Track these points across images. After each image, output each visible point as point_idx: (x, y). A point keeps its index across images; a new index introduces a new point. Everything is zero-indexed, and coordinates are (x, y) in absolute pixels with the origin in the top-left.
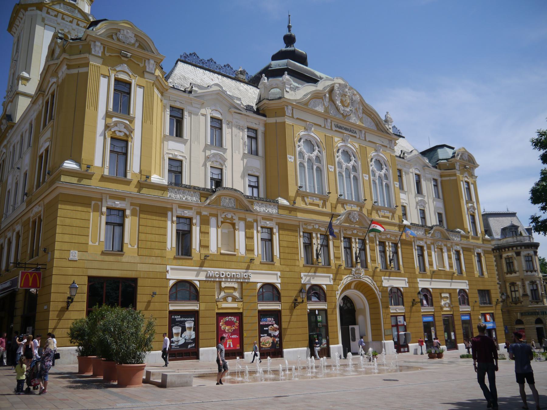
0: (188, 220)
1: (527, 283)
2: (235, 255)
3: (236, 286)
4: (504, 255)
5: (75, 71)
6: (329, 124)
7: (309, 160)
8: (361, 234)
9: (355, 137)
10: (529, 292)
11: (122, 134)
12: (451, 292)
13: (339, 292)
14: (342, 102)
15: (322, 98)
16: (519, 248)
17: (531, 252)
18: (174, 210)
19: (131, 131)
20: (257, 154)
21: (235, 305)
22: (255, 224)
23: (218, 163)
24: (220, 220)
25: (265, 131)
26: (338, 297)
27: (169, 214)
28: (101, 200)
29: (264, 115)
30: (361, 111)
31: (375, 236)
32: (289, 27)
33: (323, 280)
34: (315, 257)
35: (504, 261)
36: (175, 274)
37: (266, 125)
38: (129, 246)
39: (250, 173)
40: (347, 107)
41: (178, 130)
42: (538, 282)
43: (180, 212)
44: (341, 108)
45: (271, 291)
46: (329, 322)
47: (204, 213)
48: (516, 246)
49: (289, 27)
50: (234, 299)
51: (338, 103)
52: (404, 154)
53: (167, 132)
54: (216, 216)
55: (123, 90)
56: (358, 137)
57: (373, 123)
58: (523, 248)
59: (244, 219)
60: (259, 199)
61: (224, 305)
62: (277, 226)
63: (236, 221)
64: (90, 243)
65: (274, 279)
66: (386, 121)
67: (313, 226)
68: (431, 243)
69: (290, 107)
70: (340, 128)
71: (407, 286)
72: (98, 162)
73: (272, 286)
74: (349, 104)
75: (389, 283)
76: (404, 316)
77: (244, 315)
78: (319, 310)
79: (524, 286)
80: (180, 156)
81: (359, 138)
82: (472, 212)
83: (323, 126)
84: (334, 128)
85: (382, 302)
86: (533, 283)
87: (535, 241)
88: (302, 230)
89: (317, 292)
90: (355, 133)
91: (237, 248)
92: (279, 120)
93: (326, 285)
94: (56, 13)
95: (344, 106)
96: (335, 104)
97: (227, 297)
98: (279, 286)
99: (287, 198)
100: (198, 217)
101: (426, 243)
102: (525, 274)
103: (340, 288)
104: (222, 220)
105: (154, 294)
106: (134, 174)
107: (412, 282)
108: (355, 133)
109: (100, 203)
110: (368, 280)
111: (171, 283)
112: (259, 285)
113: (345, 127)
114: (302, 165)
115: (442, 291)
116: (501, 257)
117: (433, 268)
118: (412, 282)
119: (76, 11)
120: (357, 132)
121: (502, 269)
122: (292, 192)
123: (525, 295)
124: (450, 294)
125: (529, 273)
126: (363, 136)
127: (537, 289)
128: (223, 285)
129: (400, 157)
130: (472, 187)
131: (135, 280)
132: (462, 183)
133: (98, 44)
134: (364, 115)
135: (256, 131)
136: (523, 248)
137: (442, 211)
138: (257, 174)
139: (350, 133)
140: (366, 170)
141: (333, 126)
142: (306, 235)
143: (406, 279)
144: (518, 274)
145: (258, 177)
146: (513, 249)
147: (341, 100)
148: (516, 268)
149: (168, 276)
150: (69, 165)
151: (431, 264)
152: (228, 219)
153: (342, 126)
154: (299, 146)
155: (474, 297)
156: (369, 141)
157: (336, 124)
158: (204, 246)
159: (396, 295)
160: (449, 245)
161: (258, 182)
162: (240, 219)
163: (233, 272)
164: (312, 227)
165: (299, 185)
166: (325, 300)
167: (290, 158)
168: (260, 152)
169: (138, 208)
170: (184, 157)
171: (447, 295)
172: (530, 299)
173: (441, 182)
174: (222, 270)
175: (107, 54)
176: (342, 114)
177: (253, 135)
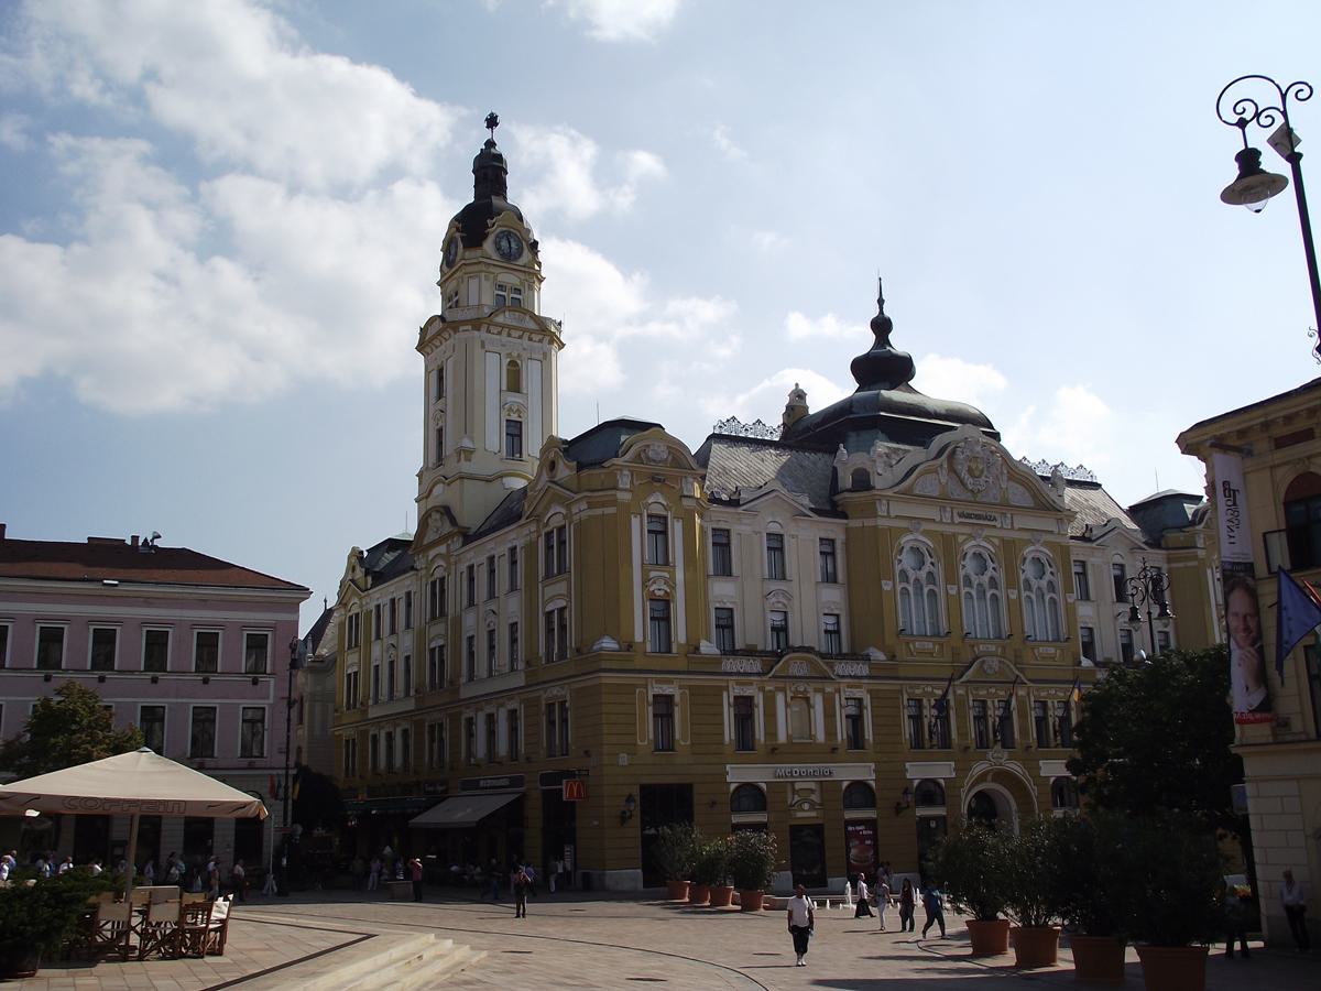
5: (599, 511)
6: (948, 515)
8: (1002, 693)
11: (662, 593)
13: (966, 788)
14: (970, 471)
15: (936, 472)
18: (730, 689)
19: (673, 588)
20: (835, 581)
21: (814, 814)
23: (780, 605)
24: (790, 694)
25: (847, 539)
27: (725, 694)
28: (646, 686)
29: (846, 517)
30: (1005, 478)
31: (1028, 694)
32: (881, 302)
33: (942, 771)
34: (927, 737)
36: (737, 775)
37: (847, 530)
38: (683, 743)
39: (826, 612)
40: (979, 477)
44: (969, 481)
45: (860, 793)
47: (767, 688)
49: (881, 302)
50: (812, 808)
51: (965, 475)
52: (1091, 530)
54: (783, 690)
55: (660, 531)
56: (998, 524)
59: (822, 691)
60: (842, 656)
61: (799, 814)
64: (639, 743)
65: (864, 772)
70: (969, 516)
72: (638, 638)
74: (982, 472)
81: (1002, 528)
84: (957, 520)
88: (906, 697)
89: (930, 793)
90: (995, 519)
91: (813, 733)
92: (869, 523)
94: (500, 329)
95: (973, 476)
96: (959, 476)
98: (873, 784)
100: (761, 696)
103: (967, 783)
105: (714, 803)
106: (679, 645)
109: (645, 691)
110: (1016, 767)
111: (733, 787)
112: (845, 784)
114: (905, 591)
119: (528, 318)
126: (1009, 521)
128: (797, 786)
131: (690, 787)
134: (1011, 483)
135: (832, 541)
138: (836, 612)
141: (955, 514)
142: (912, 703)
145: (837, 616)
147: (969, 467)
150: (608, 644)
152: (801, 693)
156: (1020, 529)
157: (960, 511)
158: (771, 731)
161: (838, 623)
162: (816, 691)
163: (812, 767)
168: (841, 576)
169: (687, 691)
170: (734, 603)
173: (1170, 571)
174: (796, 767)
176: (972, 491)
177: (828, 549)
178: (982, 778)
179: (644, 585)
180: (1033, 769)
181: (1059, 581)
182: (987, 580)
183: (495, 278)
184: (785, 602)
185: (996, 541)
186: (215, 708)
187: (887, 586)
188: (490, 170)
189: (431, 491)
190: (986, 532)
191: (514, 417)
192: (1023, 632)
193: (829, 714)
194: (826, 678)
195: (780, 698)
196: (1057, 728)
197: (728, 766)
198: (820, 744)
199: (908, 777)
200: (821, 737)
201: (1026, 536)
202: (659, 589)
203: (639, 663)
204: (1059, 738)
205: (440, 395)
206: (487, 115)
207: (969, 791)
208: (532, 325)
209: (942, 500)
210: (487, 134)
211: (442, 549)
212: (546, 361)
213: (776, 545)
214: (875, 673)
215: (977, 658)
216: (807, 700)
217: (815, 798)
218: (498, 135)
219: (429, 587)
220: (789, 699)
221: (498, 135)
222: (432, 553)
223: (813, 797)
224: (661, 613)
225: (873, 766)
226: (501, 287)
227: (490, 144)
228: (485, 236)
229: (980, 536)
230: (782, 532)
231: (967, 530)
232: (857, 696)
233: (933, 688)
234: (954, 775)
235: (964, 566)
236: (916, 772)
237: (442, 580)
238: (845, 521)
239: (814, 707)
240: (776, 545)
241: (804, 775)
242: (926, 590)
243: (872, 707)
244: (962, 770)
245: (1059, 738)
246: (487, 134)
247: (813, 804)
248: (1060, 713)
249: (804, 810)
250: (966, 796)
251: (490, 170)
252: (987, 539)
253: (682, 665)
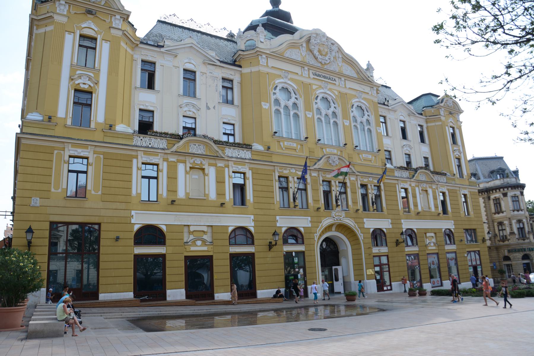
0: (155, 167)
1: (514, 222)
2: (205, 199)
3: (205, 229)
4: (492, 197)
7: (286, 107)
9: (335, 84)
10: (516, 231)
12: (436, 232)
13: (318, 234)
14: (319, 51)
15: (299, 48)
16: (506, 189)
17: (517, 192)
19: (97, 83)
20: (232, 103)
21: (205, 248)
22: (226, 169)
24: (189, 165)
25: (241, 80)
26: (316, 239)
27: (135, 161)
28: (63, 149)
31: (357, 179)
33: (301, 223)
34: (291, 200)
35: (492, 202)
38: (93, 192)
39: (225, 121)
40: (325, 56)
41: (150, 83)
42: (524, 220)
43: (145, 159)
45: (243, 234)
46: (307, 263)
48: (503, 188)
51: (316, 52)
52: (388, 101)
53: (138, 84)
54: (185, 162)
56: (337, 83)
57: (353, 72)
58: (510, 189)
59: (215, 165)
61: (193, 249)
62: (250, 171)
63: (206, 167)
64: (53, 190)
65: (247, 221)
66: (368, 69)
67: (290, 170)
68: (416, 186)
69: (264, 56)
70: (319, 76)
71: (391, 227)
72: (61, 113)
73: (244, 229)
74: (327, 54)
75: (372, 223)
76: (387, 256)
77: (214, 258)
78: (297, 253)
79: (511, 225)
80: (151, 106)
82: (457, 156)
83: (300, 73)
84: (312, 76)
85: (364, 243)
86: (519, 221)
87: (522, 182)
89: (294, 234)
91: (207, 192)
92: (254, 69)
93: (303, 227)
95: (321, 55)
97: (196, 240)
98: (252, 229)
99: (261, 143)
100: (165, 164)
101: (410, 185)
102: (512, 213)
103: (319, 231)
104: (191, 166)
105: (117, 239)
106: (97, 123)
107: (396, 222)
108: (335, 80)
109: (62, 152)
110: (350, 222)
111: (136, 227)
113: (323, 75)
114: (278, 112)
116: (489, 198)
117: (418, 209)
118: (396, 222)
120: (337, 79)
121: (490, 209)
122: (267, 138)
123: (512, 233)
124: (435, 233)
125: (516, 212)
127: (524, 227)
128: (192, 229)
129: (384, 104)
132: (447, 128)
134: (344, 64)
136: (510, 189)
137: (428, 156)
139: (329, 81)
140: (346, 116)
143: (390, 220)
144: (505, 214)
145: (233, 125)
146: (500, 191)
147: (319, 49)
148: (503, 209)
149: (133, 221)
151: (416, 205)
153: (320, 74)
154: (274, 94)
155: (460, 235)
157: (314, 72)
159: (378, 236)
160: (434, 187)
162: (210, 165)
164: (288, 171)
165: (274, 131)
166: (303, 243)
167: (265, 105)
168: (236, 102)
169: (102, 156)
171: (433, 235)
172: (517, 236)
173: (427, 128)
175: (73, 12)
178: (329, 228)
179: (71, 79)
181: (372, 119)
182: (331, 113)
184: (195, 111)
185: (336, 93)
187: (265, 106)
190: (330, 86)
192: (353, 144)
193: (220, 182)
194: (221, 158)
195: (181, 168)
196: (374, 200)
197: (133, 213)
198: (213, 201)
199: (278, 225)
200: (213, 195)
201: (353, 93)
202: (84, 84)
203: (59, 131)
204: (375, 206)
207: (321, 236)
209: (302, 64)
213: (190, 76)
214: (255, 157)
215: (325, 155)
217: (207, 237)
220: (188, 169)
223: (205, 237)
224: (83, 99)
225: (252, 217)
229: (326, 88)
230: (195, 69)
231: (319, 83)
232: (241, 170)
233: (296, 170)
234: (310, 225)
235: (316, 103)
236: (284, 223)
239: (207, 175)
240: (190, 76)
241: (199, 221)
242: (292, 113)
243: (253, 179)
244: (316, 222)
245: (375, 206)
247: (204, 242)
248: (375, 192)
249: (197, 246)
250: (319, 239)
252: (330, 90)
253: (99, 136)
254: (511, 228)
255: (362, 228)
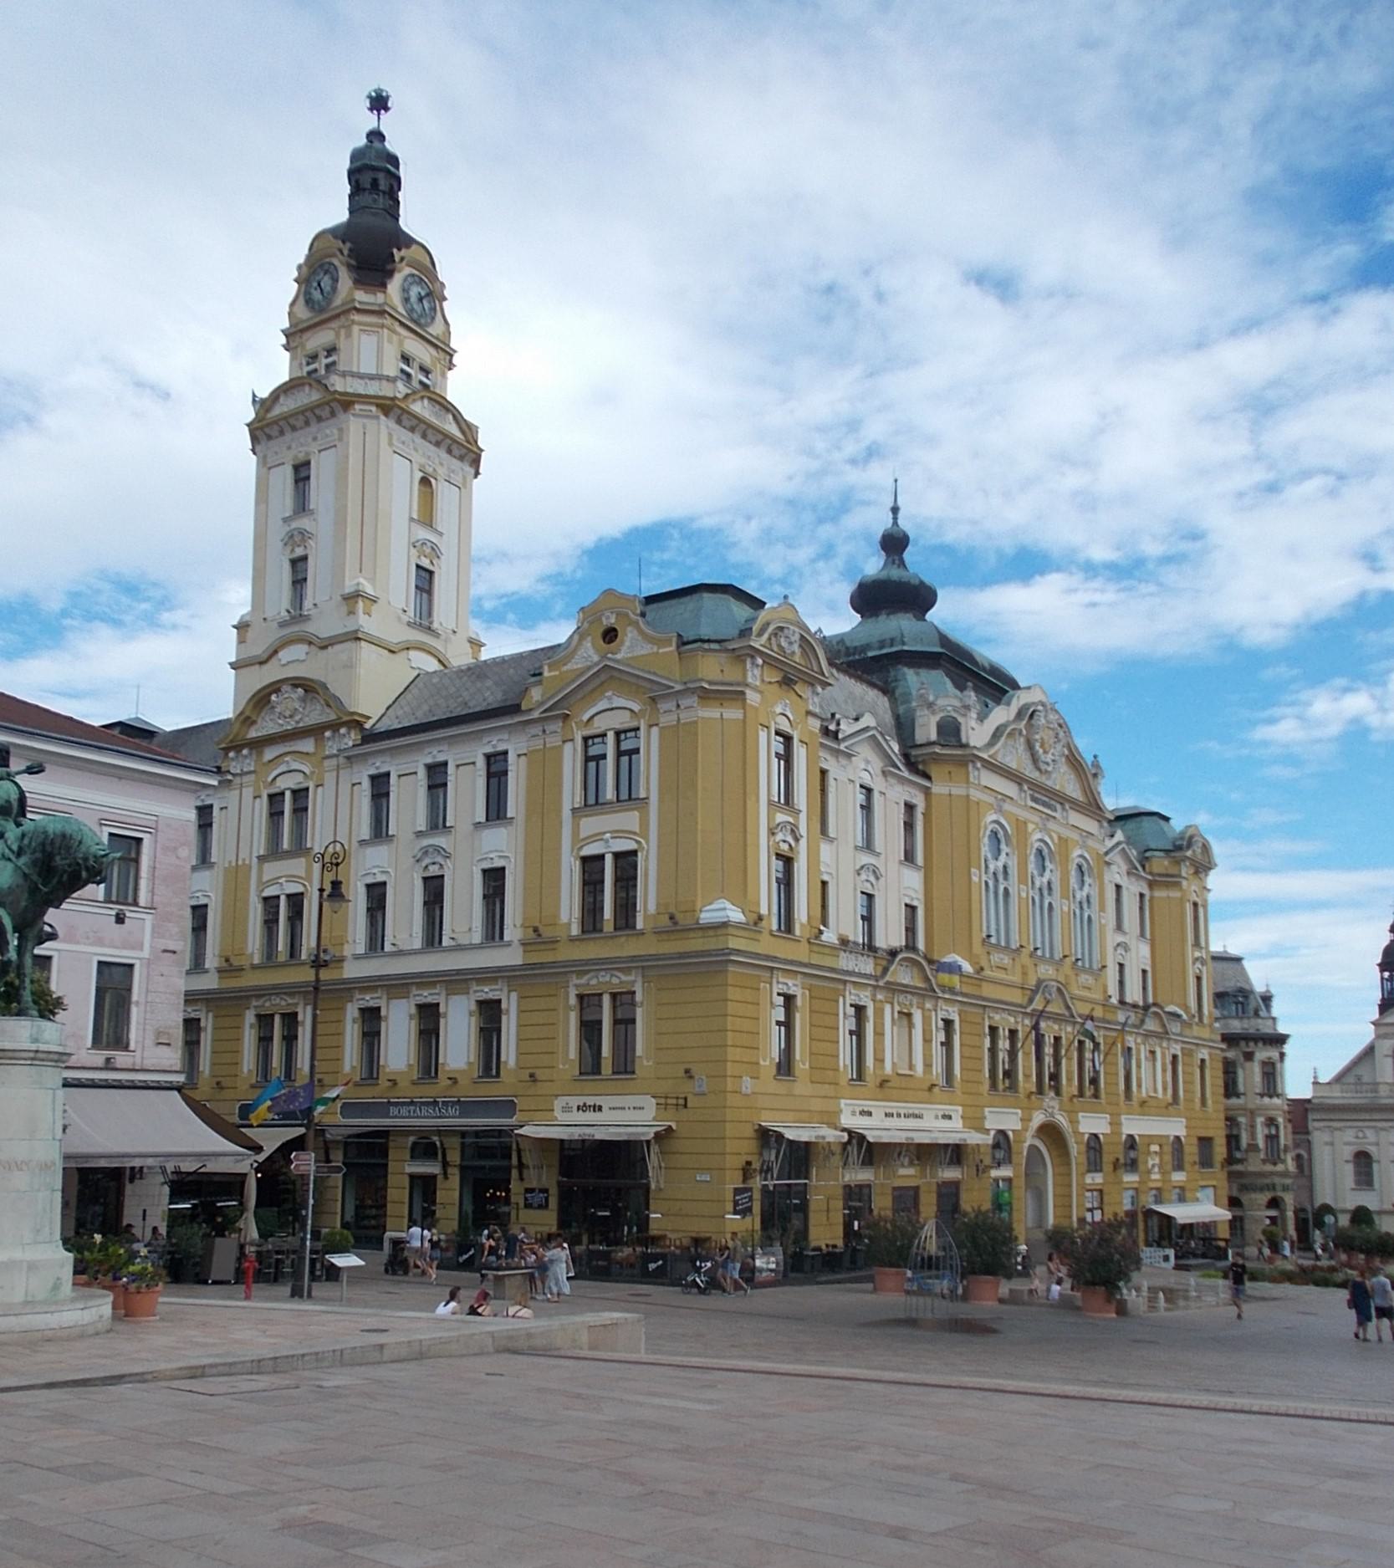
1: (1260, 1120)
10: (1261, 1143)
16: (1252, 1044)
17: (1273, 1054)
42: (1280, 1120)
58: (1260, 1044)
75: (1093, 1123)
76: (1101, 1191)
79: (1253, 1127)
86: (1271, 1122)
87: (1282, 1029)
92: (958, 790)
102: (1258, 1101)
107: (1115, 1124)
115: (1151, 1139)
118: (1115, 1124)
119: (451, 417)
123: (1253, 1147)
125: (1266, 1100)
127: (1277, 1136)
130: (1201, 910)
133: (760, 661)
136: (1260, 1044)
137: (1148, 968)
144: (1241, 1101)
148: (1241, 1088)
172: (1262, 1156)
180: (1074, 1122)
183: (401, 343)
186: (131, 966)
188: (374, 177)
189: (276, 652)
191: (425, 563)
195: (888, 1008)
205: (302, 505)
206: (370, 88)
208: (453, 430)
210: (370, 121)
211: (307, 745)
212: (463, 487)
216: (909, 1015)
218: (388, 123)
219: (263, 804)
221: (388, 123)
222: (270, 753)
226: (406, 359)
227: (376, 136)
228: (390, 274)
237: (300, 794)
238: (928, 784)
244: (1026, 1120)
246: (370, 121)
251: (374, 177)
254: (1253, 1135)
255: (1076, 1132)
